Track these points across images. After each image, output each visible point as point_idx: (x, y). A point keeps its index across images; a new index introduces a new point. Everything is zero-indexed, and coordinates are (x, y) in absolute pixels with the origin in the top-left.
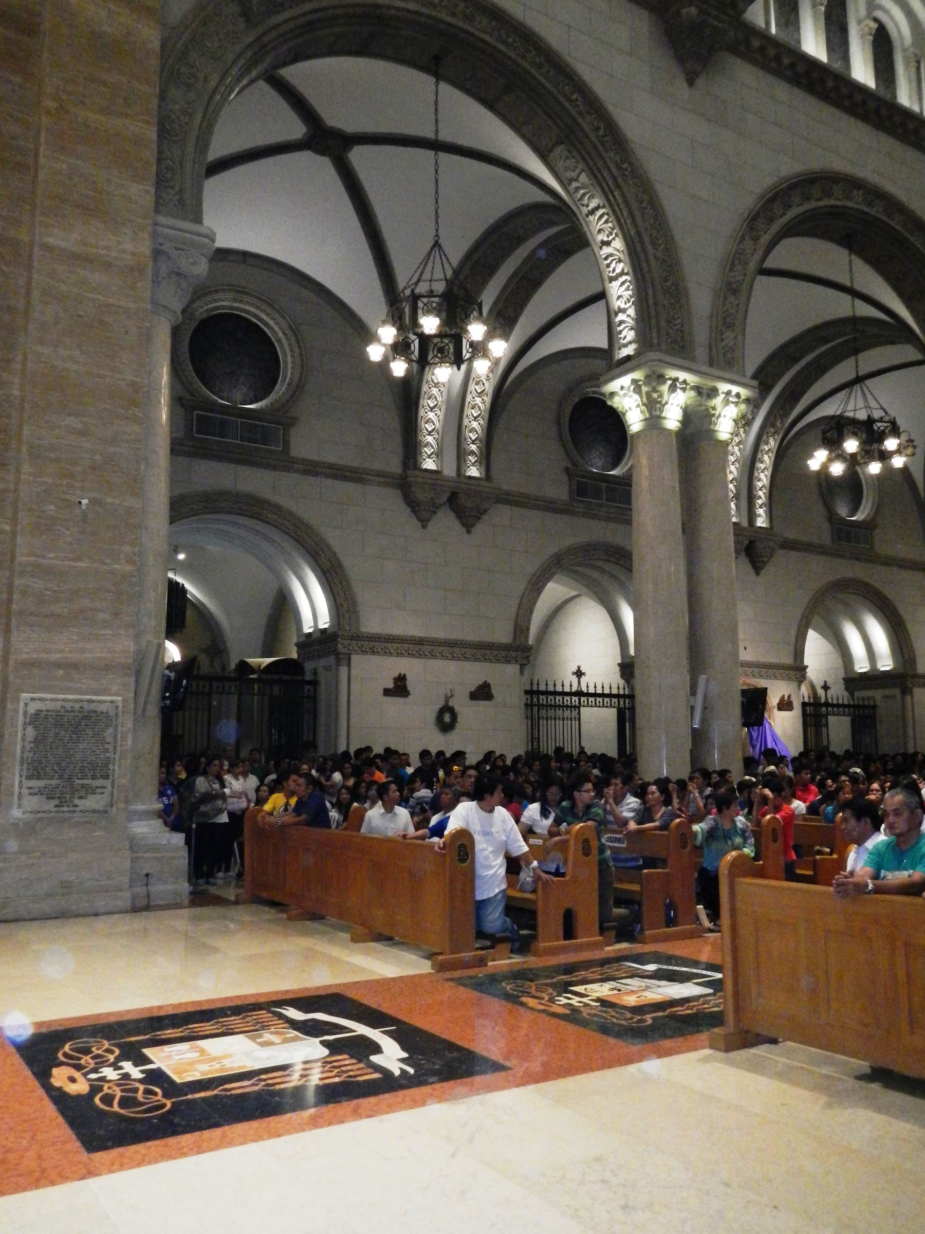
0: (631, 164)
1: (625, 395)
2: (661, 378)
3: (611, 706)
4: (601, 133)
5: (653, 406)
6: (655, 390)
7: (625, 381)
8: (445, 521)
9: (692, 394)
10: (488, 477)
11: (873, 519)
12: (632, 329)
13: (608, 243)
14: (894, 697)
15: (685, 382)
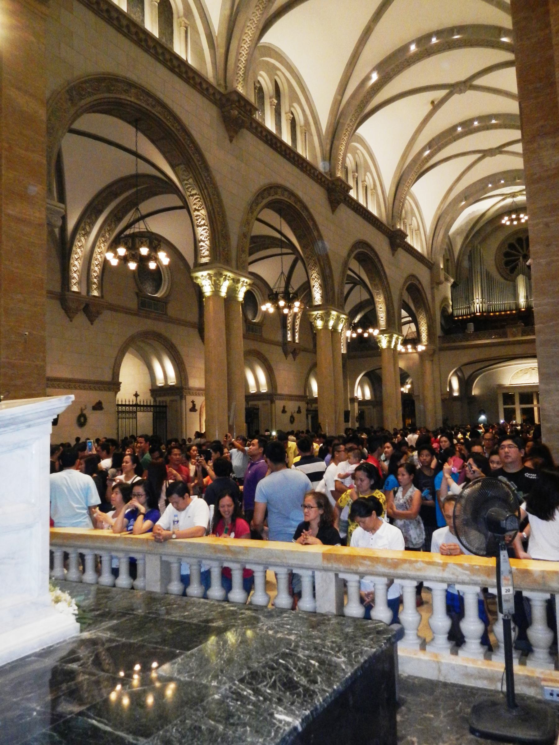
0: (211, 178)
1: (203, 279)
2: (221, 275)
3: (151, 411)
4: (200, 163)
5: (216, 286)
6: (218, 280)
7: (205, 273)
8: (81, 319)
9: (231, 281)
10: (102, 297)
11: (263, 321)
12: (207, 250)
13: (198, 210)
14: (266, 404)
15: (229, 277)
